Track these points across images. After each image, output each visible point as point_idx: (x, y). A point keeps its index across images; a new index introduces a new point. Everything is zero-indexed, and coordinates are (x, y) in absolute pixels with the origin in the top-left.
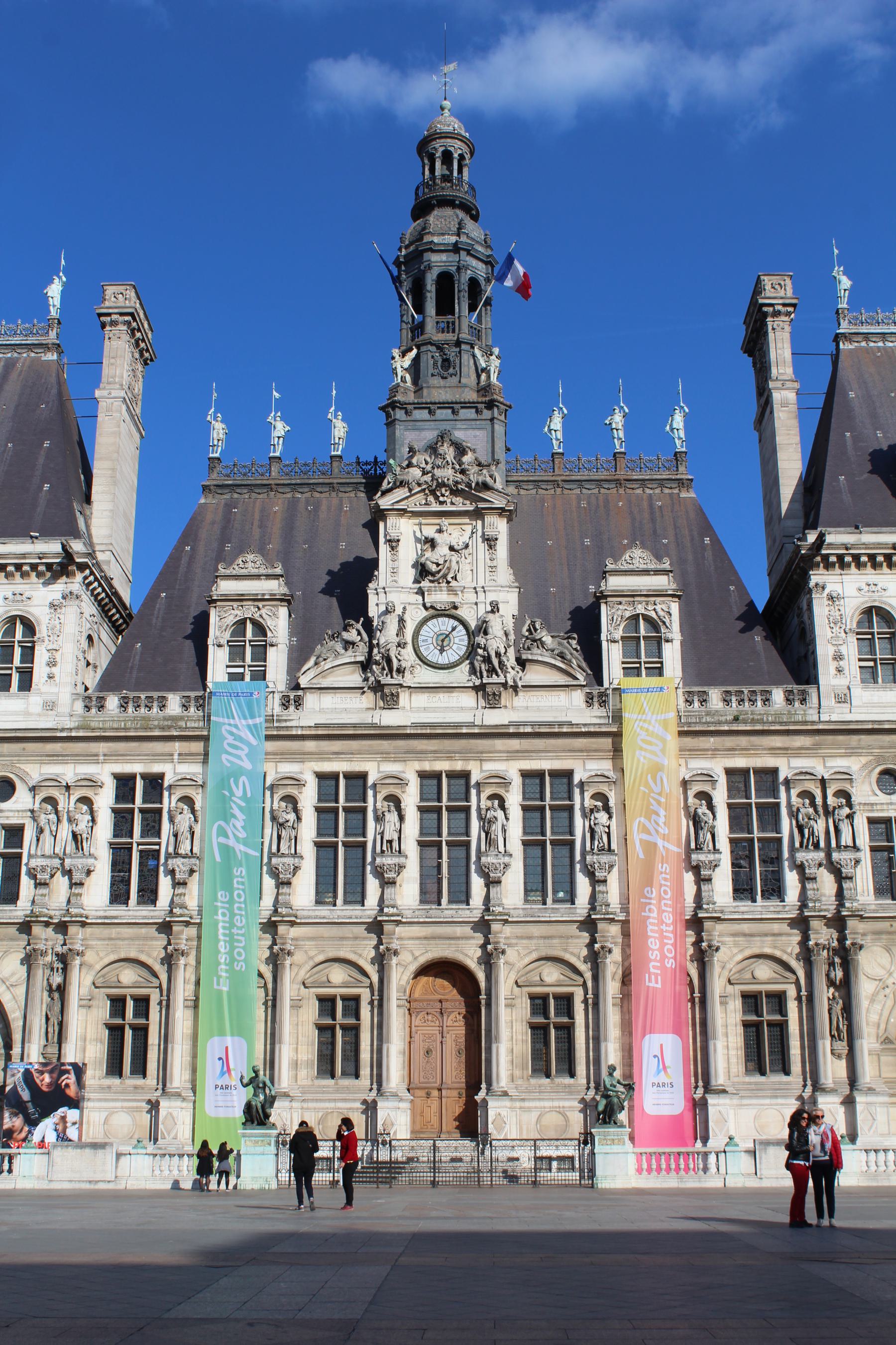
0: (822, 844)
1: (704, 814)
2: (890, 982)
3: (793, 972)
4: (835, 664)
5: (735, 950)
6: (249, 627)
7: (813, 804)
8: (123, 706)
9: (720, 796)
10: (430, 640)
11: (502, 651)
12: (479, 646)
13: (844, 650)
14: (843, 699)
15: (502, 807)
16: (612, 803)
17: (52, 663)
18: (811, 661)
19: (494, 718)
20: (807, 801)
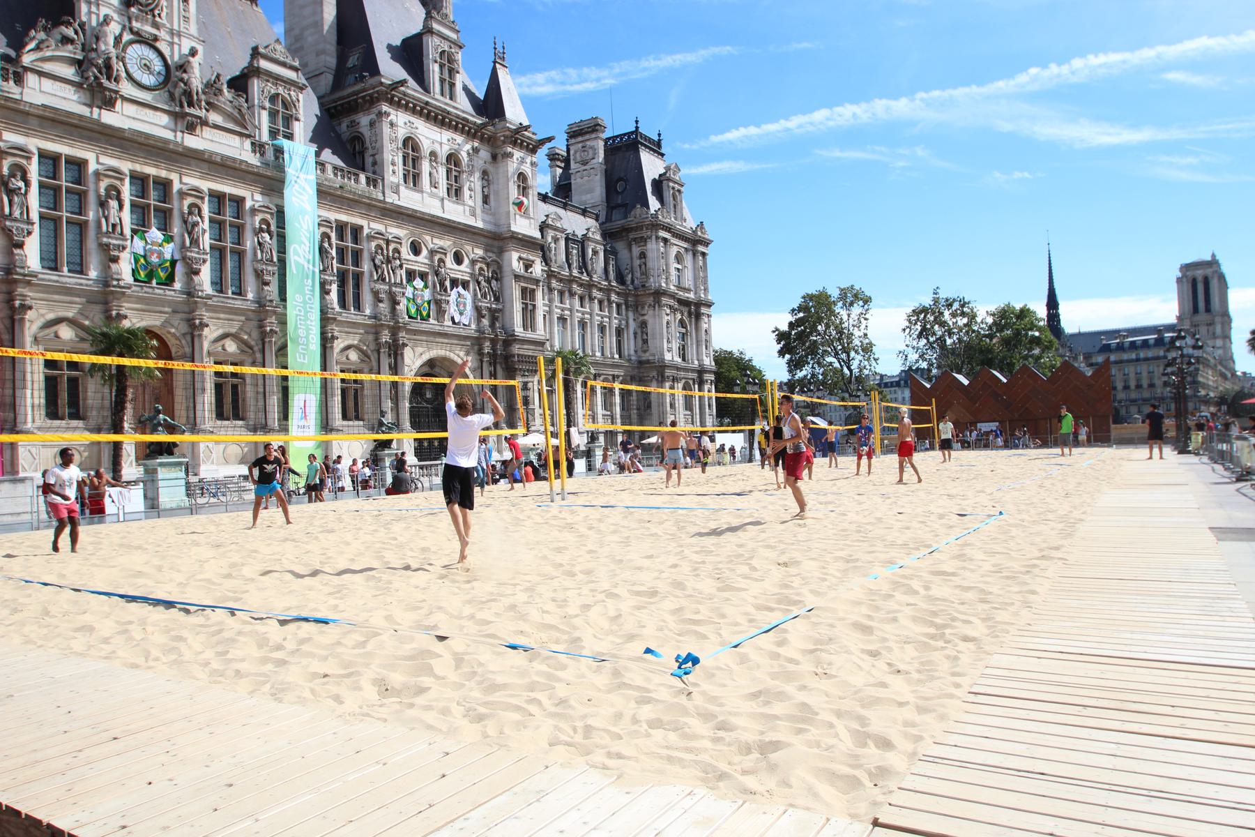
0: (387, 280)
2: (413, 367)
3: (369, 358)
4: (391, 167)
7: (383, 255)
9: (333, 235)
10: (134, 61)
11: (200, 90)
12: (182, 80)
13: (396, 158)
14: (397, 192)
15: (200, 215)
16: (273, 228)
18: (369, 160)
19: (191, 142)
20: (380, 251)
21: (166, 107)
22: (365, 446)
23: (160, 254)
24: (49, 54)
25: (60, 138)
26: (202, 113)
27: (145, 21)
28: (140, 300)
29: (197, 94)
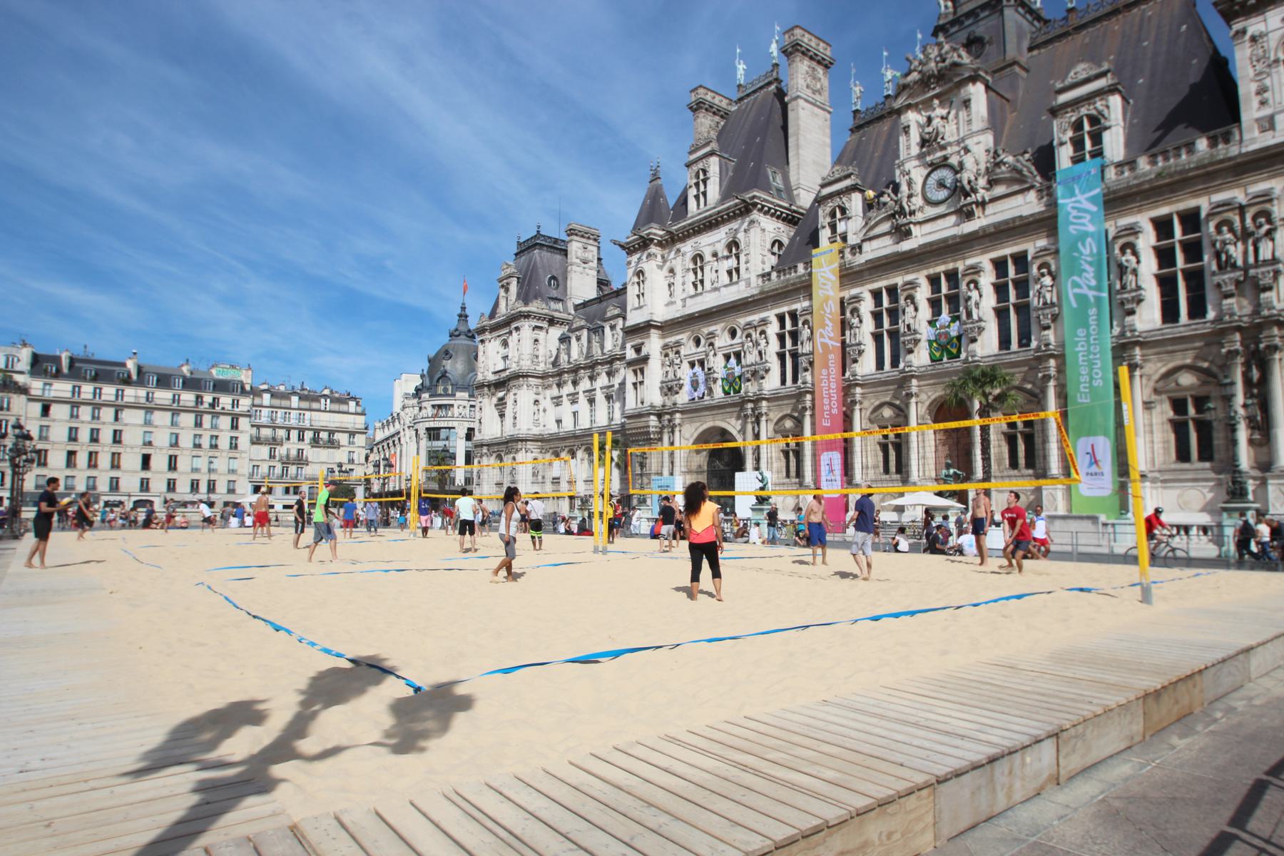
0: (1240, 263)
1: (1127, 261)
4: (1259, 98)
5: (1159, 365)
6: (837, 210)
7: (1231, 230)
8: (779, 277)
11: (973, 178)
13: (1268, 82)
15: (976, 287)
17: (747, 262)
19: (970, 227)
20: (1225, 229)
21: (952, 210)
22: (1210, 496)
23: (947, 334)
24: (873, 223)
25: (880, 278)
26: (982, 194)
27: (934, 151)
28: (932, 376)
29: (969, 182)
